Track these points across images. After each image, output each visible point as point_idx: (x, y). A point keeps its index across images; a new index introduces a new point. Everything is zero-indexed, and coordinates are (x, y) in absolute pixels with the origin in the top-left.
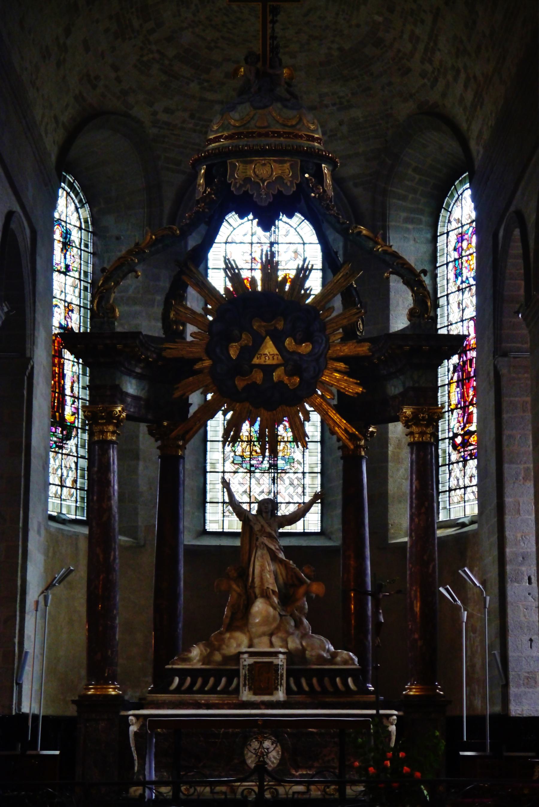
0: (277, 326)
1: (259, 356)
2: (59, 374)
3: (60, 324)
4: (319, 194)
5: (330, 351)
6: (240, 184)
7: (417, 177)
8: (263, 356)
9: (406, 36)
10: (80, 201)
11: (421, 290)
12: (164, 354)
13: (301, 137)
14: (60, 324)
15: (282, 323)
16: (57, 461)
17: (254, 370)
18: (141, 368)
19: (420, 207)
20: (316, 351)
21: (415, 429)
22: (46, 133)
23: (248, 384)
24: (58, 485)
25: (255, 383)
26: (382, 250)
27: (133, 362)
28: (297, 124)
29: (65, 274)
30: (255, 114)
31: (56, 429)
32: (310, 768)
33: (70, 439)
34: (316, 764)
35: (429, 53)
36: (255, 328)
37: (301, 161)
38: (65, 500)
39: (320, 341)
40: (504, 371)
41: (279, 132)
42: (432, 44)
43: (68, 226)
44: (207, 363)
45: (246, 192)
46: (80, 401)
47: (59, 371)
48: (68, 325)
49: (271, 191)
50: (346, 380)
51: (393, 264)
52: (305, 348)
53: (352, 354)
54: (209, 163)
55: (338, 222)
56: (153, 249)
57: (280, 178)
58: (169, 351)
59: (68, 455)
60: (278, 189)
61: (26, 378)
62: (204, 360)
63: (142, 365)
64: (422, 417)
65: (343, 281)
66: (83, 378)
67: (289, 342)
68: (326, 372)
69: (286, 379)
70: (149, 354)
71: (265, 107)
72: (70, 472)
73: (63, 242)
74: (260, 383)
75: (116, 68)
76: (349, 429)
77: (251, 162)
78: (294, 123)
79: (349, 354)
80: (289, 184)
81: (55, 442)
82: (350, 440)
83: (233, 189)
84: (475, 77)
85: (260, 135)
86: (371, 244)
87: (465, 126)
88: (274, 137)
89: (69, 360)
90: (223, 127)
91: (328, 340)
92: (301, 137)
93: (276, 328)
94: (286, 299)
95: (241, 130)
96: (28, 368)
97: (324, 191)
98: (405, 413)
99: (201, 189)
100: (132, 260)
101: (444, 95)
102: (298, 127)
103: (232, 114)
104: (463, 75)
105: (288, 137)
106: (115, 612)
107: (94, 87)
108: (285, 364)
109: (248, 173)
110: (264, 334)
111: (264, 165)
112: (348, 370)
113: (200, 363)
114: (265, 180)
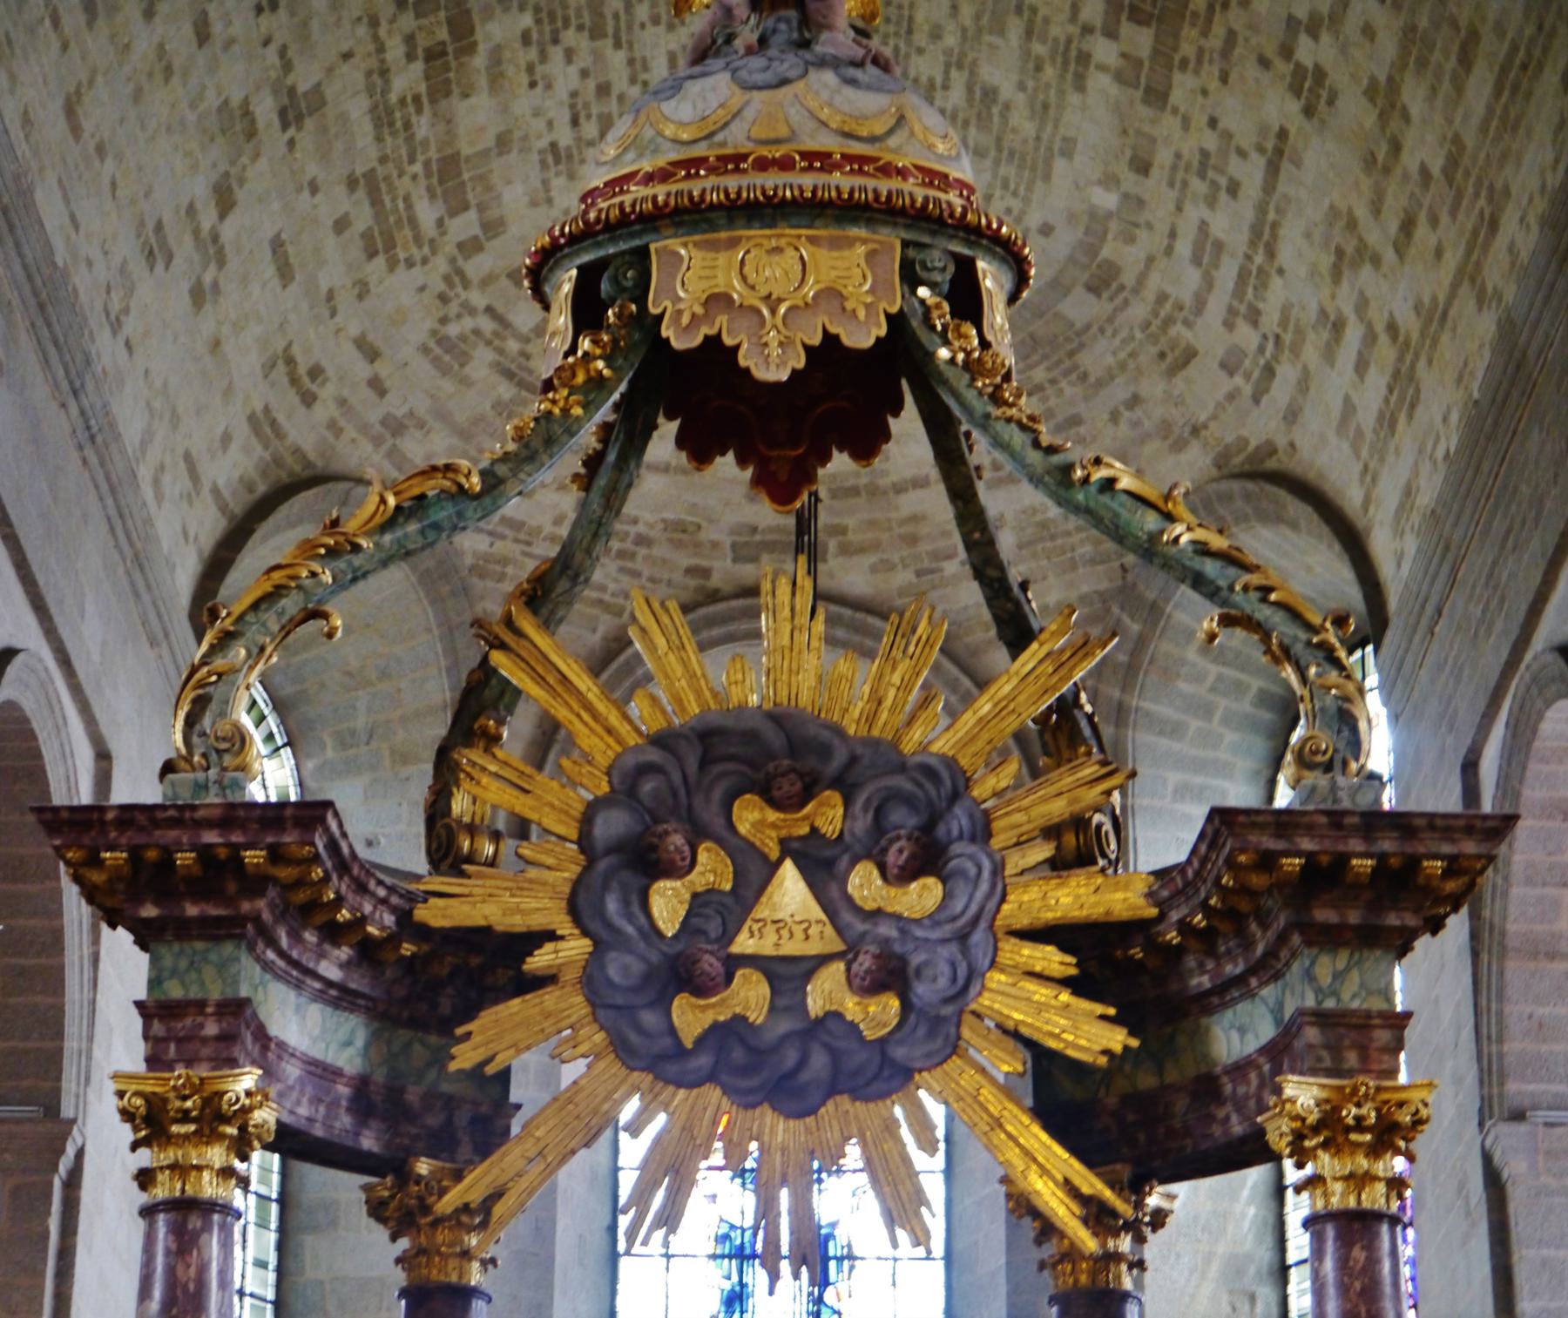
0: (819, 823)
1: (756, 927)
4: (968, 354)
5: (1006, 907)
6: (693, 315)
7: (1214, 670)
8: (770, 930)
9: (1184, 248)
10: (270, 737)
11: (1333, 676)
12: (422, 913)
13: (902, 173)
15: (840, 811)
17: (739, 973)
18: (343, 966)
19: (1223, 755)
20: (958, 905)
21: (1325, 1163)
22: (159, 497)
23: (715, 1027)
25: (740, 1019)
26: (1194, 542)
27: (310, 937)
28: (891, 132)
30: (747, 103)
35: (1250, 291)
36: (743, 828)
37: (905, 244)
39: (973, 871)
40: (1514, 1168)
41: (829, 155)
42: (1259, 259)
44: (575, 948)
45: (713, 342)
46: (247, 1300)
49: (800, 335)
50: (1067, 1006)
51: (1231, 588)
52: (923, 896)
53: (1085, 913)
54: (586, 258)
55: (1036, 444)
56: (387, 538)
57: (832, 295)
58: (440, 902)
60: (825, 330)
61: (57, 1184)
62: (562, 938)
63: (344, 953)
64: (1359, 1119)
65: (1050, 670)
66: (258, 1237)
67: (864, 884)
68: (996, 979)
69: (851, 1006)
70: (368, 908)
71: (784, 82)
74: (759, 1021)
76: (1077, 1181)
77: (733, 244)
78: (879, 129)
79: (1076, 913)
80: (862, 314)
82: (1085, 1221)
83: (666, 331)
84: (1392, 328)
85: (763, 165)
86: (1151, 521)
87: (1351, 497)
88: (810, 168)
90: (634, 144)
91: (998, 869)
92: (902, 173)
93: (814, 830)
94: (851, 731)
95: (699, 151)
96: (62, 1151)
97: (985, 344)
98: (1292, 1101)
99: (560, 344)
100: (314, 574)
101: (1292, 415)
102: (893, 142)
103: (668, 107)
104: (1353, 334)
105: (861, 172)
107: (308, 399)
108: (849, 955)
109: (721, 280)
110: (774, 854)
111: (778, 250)
112: (1073, 971)
113: (549, 947)
114: (780, 300)
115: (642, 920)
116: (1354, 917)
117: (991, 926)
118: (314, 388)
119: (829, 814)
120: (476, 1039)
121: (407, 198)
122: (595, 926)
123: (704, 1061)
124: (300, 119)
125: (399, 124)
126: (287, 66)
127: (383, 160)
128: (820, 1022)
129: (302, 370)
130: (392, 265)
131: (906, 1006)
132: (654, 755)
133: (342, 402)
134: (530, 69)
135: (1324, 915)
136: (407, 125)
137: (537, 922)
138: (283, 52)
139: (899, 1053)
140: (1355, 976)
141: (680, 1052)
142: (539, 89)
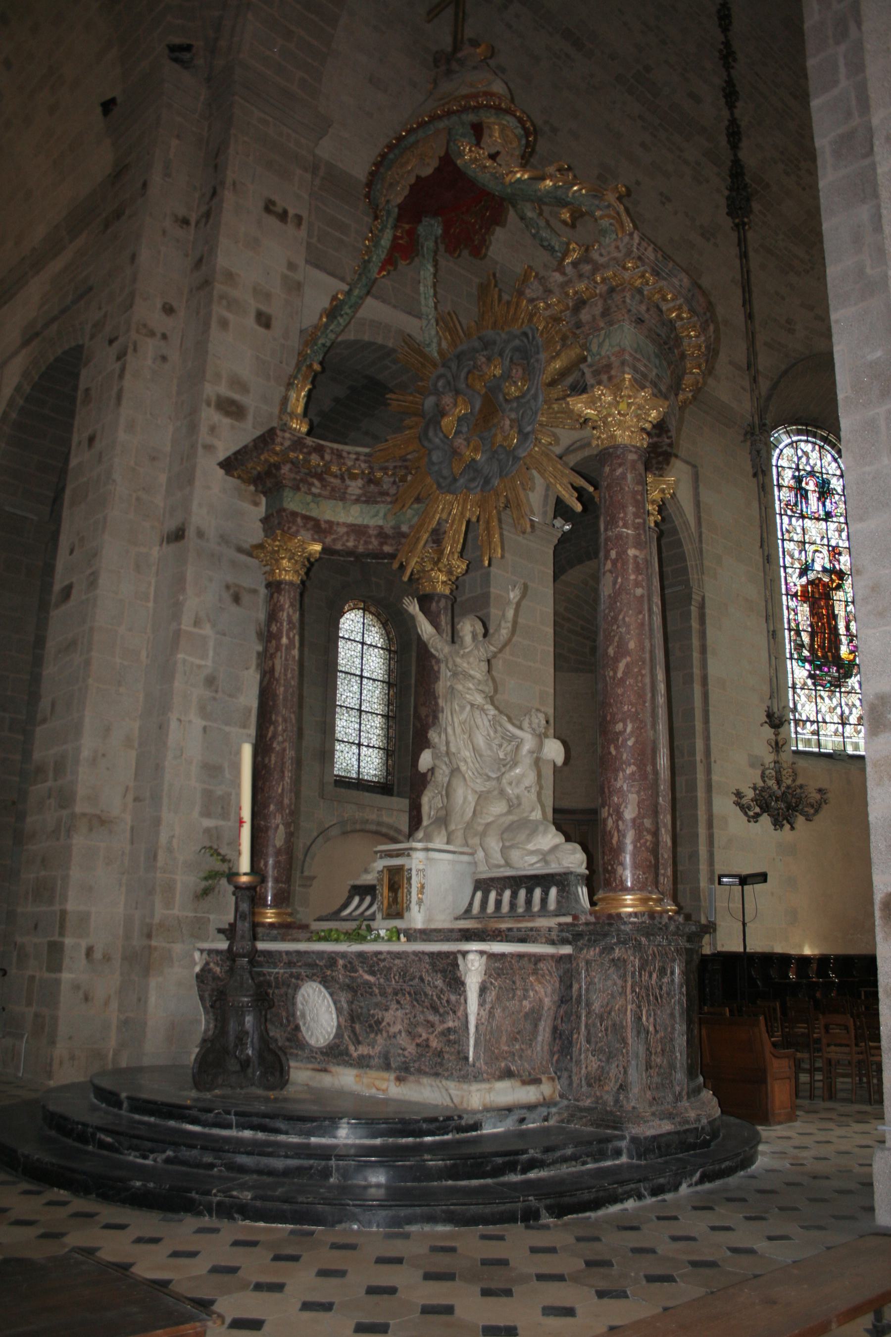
2: (828, 616)
3: (823, 567)
14: (823, 567)
16: (834, 700)
24: (838, 723)
29: (826, 520)
31: (829, 669)
33: (850, 677)
38: (848, 737)
43: (825, 476)
47: (827, 612)
59: (849, 693)
72: (854, 710)
73: (819, 492)
81: (829, 682)
89: (840, 601)
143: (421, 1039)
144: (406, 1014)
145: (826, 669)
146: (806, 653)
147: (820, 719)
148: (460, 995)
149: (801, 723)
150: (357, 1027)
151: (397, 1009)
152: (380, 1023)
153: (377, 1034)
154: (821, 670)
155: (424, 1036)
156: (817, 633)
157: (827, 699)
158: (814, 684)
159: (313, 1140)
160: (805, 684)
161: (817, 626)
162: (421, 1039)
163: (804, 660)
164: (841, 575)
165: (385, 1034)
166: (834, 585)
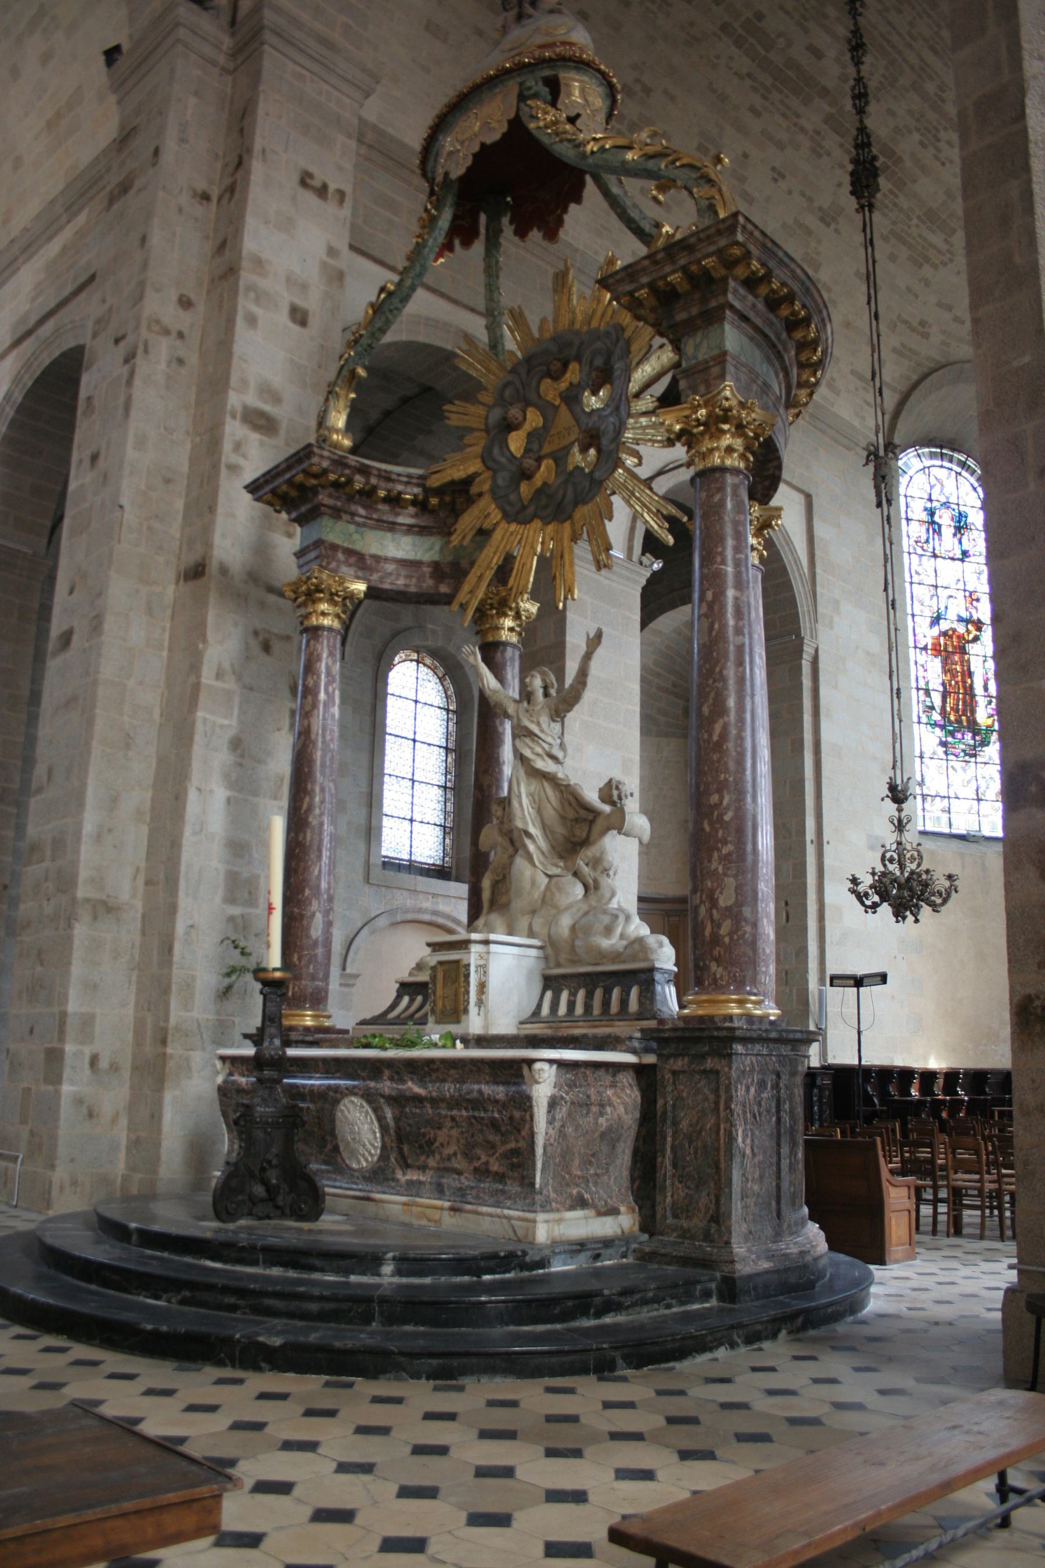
3: (959, 616)
5: (631, 385)
14: (959, 616)
29: (962, 560)
31: (963, 735)
32: (423, 1168)
34: (432, 1162)
43: (962, 508)
47: (963, 670)
48: (971, 616)
72: (991, 783)
73: (955, 527)
75: (950, 308)
81: (964, 751)
106: (307, 892)
107: (926, 336)
115: (508, 454)
116: (695, 311)
117: (627, 397)
118: (926, 330)
119: (573, 374)
120: (459, 532)
121: (920, 236)
122: (490, 464)
123: (531, 510)
124: (834, 219)
125: (891, 206)
126: (810, 200)
127: (894, 223)
128: (571, 473)
129: (915, 324)
130: (935, 267)
131: (599, 451)
132: (510, 378)
133: (944, 332)
134: (936, 158)
135: (681, 316)
136: (895, 205)
137: (472, 470)
138: (803, 194)
139: (597, 475)
140: (705, 344)
141: (524, 508)
142: (948, 165)
143: (480, 1162)
144: (462, 1133)
145: (959, 736)
146: (936, 717)
147: (952, 795)
148: (526, 1111)
149: (929, 798)
150: (406, 1148)
151: (452, 1127)
152: (432, 1143)
153: (428, 1157)
154: (954, 737)
155: (484, 1159)
156: (950, 693)
157: (959, 770)
158: (946, 753)
159: (353, 1278)
160: (934, 753)
161: (950, 685)
162: (480, 1162)
163: (935, 724)
164: (979, 625)
165: (437, 1157)
166: (971, 637)
